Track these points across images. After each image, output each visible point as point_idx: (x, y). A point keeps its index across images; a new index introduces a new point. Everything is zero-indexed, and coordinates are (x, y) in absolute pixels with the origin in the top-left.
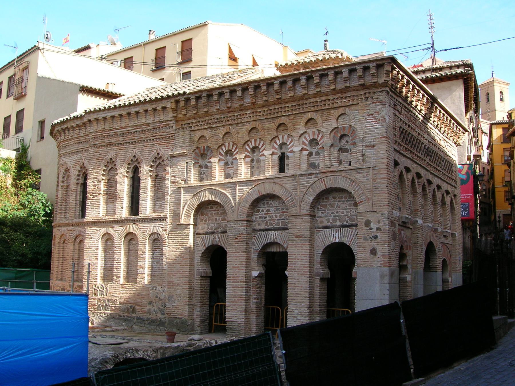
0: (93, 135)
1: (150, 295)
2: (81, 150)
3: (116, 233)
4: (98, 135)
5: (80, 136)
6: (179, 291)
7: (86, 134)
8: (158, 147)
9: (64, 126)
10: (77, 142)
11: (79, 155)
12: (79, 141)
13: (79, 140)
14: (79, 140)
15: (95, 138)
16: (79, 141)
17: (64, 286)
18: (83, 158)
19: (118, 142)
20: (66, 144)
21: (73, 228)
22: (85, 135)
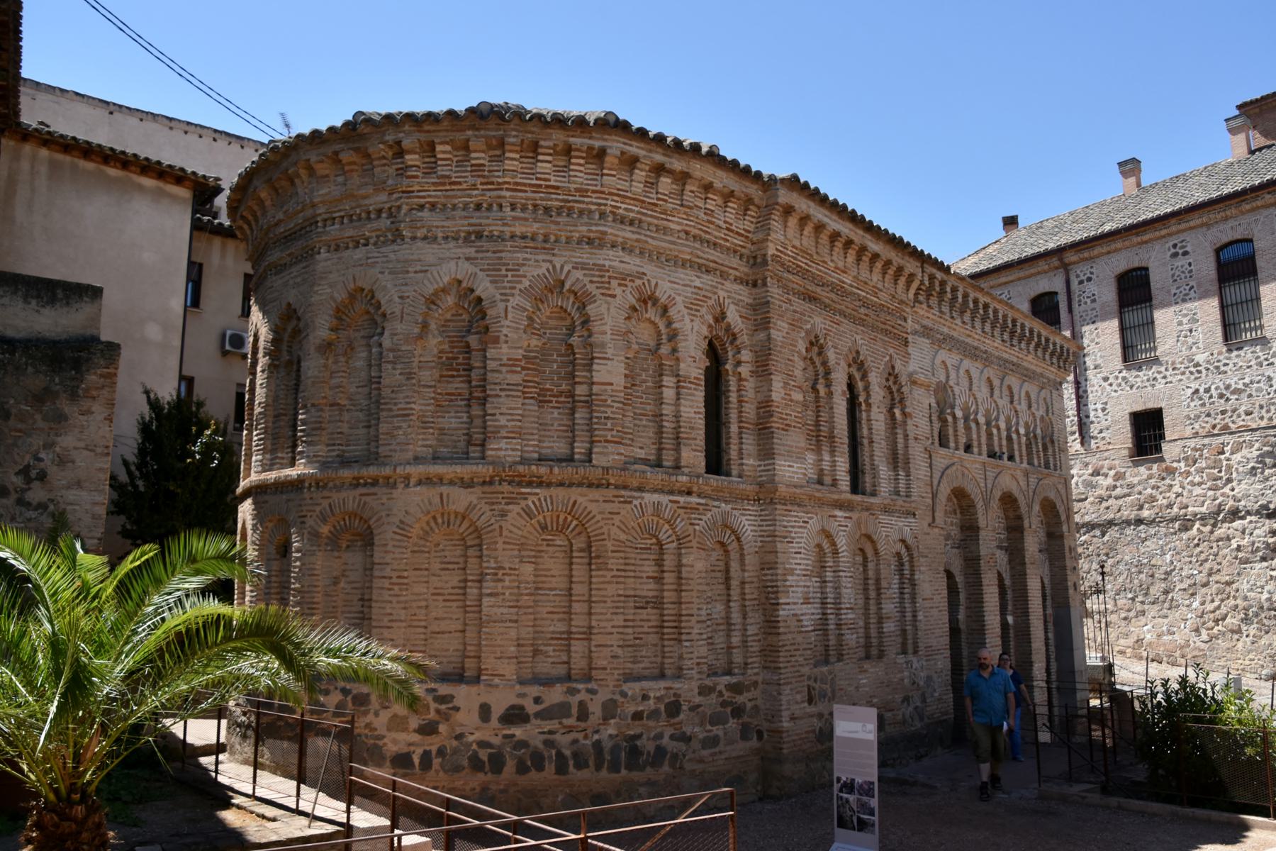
0: (777, 250)
1: (906, 681)
2: (712, 265)
3: (842, 533)
4: (789, 256)
5: (712, 223)
6: (940, 665)
7: (733, 228)
8: (891, 351)
9: (677, 164)
10: (697, 232)
11: (707, 280)
12: (703, 235)
13: (706, 232)
14: (706, 232)
15: (777, 256)
16: (703, 235)
17: (675, 695)
18: (722, 294)
19: (827, 301)
20: (639, 213)
21: (703, 501)
22: (728, 229)
